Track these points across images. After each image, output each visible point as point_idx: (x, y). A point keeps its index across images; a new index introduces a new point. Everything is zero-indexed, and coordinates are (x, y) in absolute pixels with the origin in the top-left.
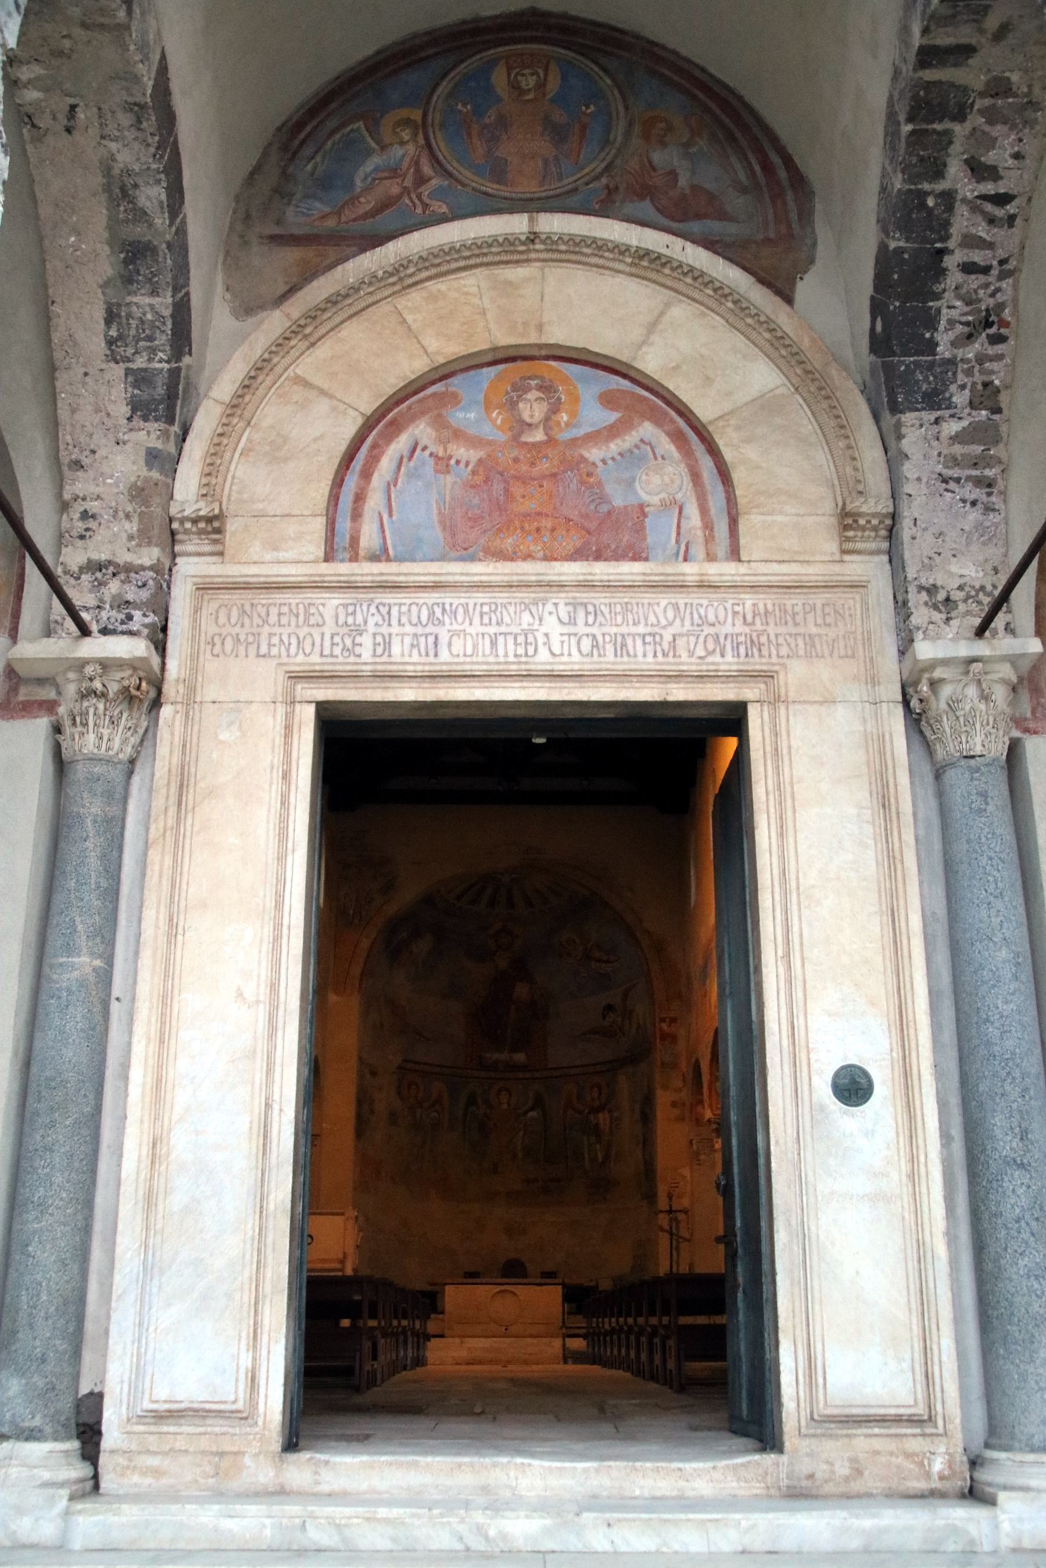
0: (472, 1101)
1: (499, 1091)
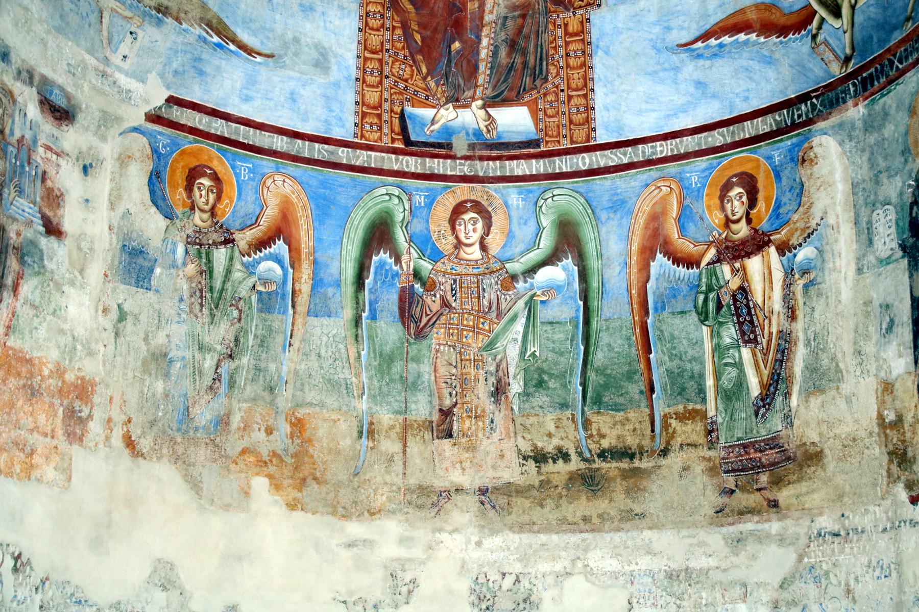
1: (458, 211)
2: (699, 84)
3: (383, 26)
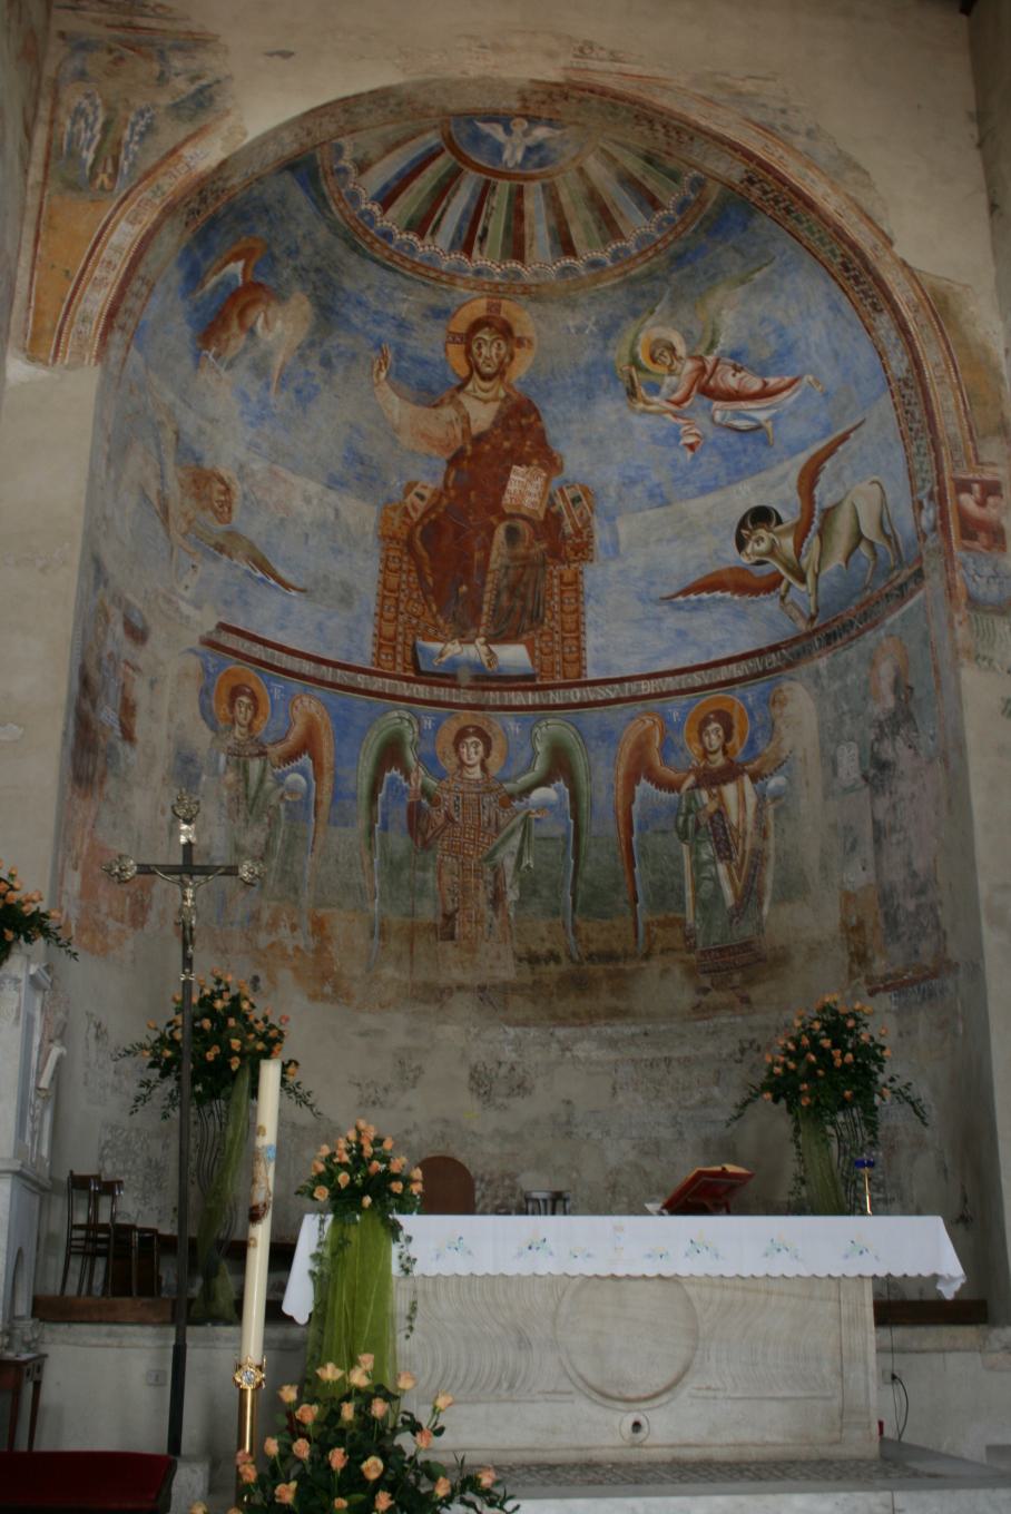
0: (391, 753)
1: (461, 735)
2: (681, 633)
3: (401, 568)
